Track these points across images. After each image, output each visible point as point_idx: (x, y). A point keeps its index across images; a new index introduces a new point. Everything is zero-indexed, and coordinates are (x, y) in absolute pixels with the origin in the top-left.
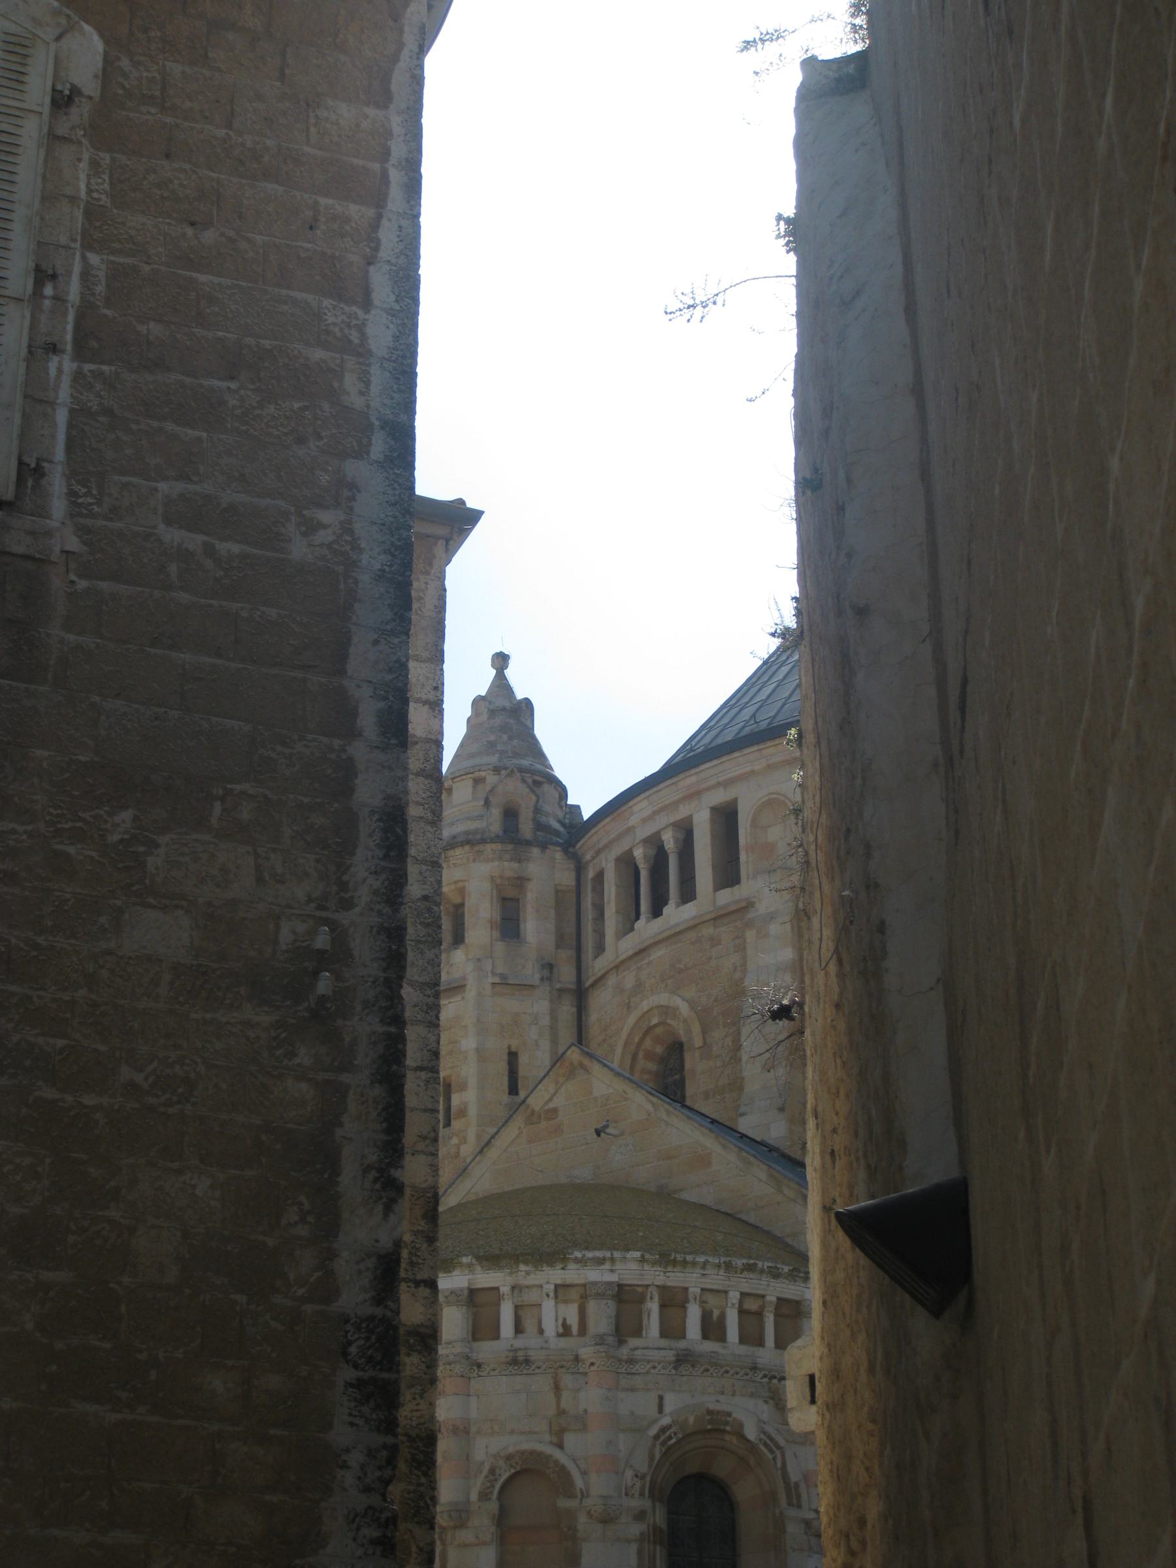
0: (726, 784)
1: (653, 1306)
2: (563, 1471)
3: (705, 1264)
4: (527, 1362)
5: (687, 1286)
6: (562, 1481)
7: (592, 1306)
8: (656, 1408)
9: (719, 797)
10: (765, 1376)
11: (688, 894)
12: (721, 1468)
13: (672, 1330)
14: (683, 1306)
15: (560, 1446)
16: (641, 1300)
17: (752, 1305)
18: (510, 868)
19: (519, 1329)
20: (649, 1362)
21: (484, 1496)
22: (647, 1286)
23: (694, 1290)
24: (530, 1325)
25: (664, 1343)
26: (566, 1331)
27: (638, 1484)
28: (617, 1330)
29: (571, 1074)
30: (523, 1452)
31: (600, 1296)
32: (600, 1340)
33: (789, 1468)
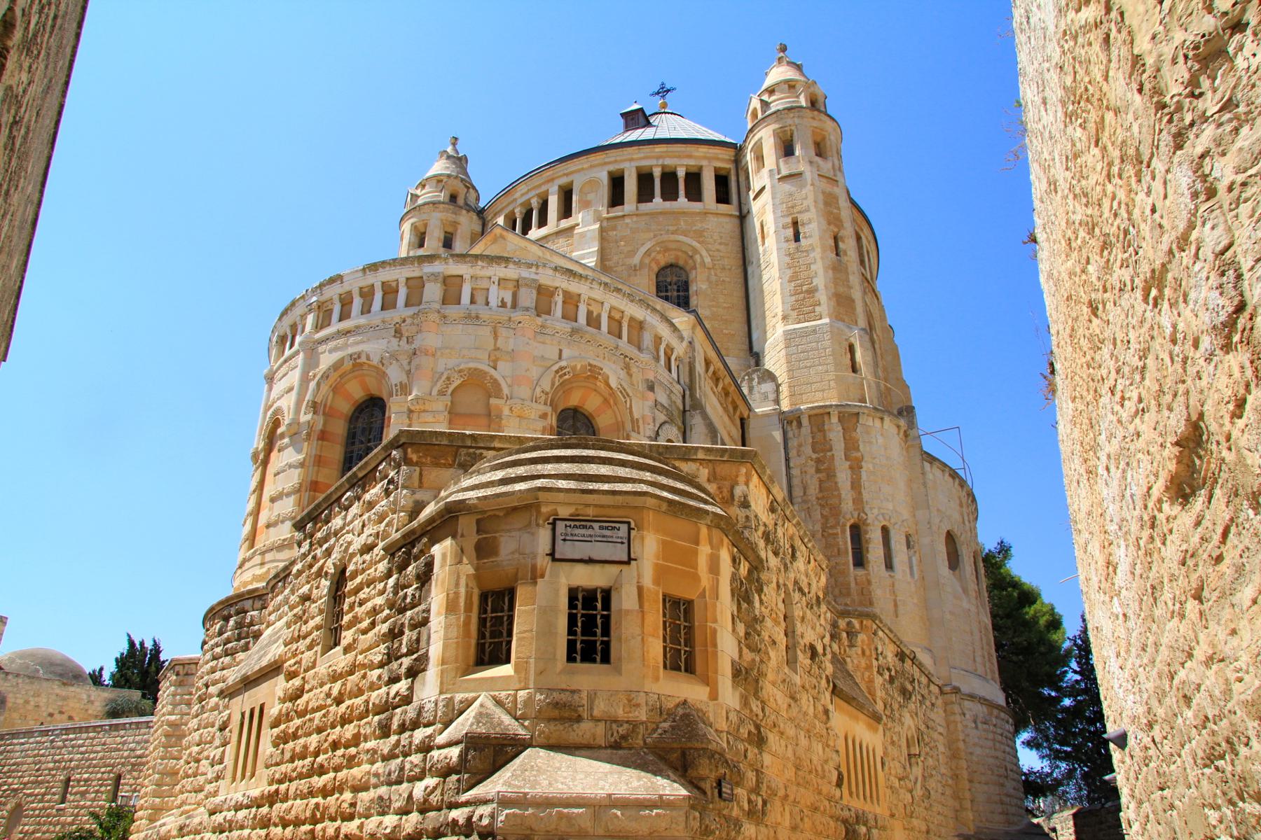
0: (567, 175)
1: (559, 299)
2: (496, 383)
4: (477, 317)
6: (493, 389)
7: (523, 292)
9: (564, 181)
11: (543, 222)
12: (591, 404)
13: (569, 316)
17: (617, 316)
18: (451, 217)
19: (473, 302)
21: (442, 393)
24: (480, 299)
26: (503, 305)
27: (543, 398)
28: (536, 308)
29: (495, 241)
30: (470, 369)
31: (526, 285)
32: (527, 309)
33: (634, 409)
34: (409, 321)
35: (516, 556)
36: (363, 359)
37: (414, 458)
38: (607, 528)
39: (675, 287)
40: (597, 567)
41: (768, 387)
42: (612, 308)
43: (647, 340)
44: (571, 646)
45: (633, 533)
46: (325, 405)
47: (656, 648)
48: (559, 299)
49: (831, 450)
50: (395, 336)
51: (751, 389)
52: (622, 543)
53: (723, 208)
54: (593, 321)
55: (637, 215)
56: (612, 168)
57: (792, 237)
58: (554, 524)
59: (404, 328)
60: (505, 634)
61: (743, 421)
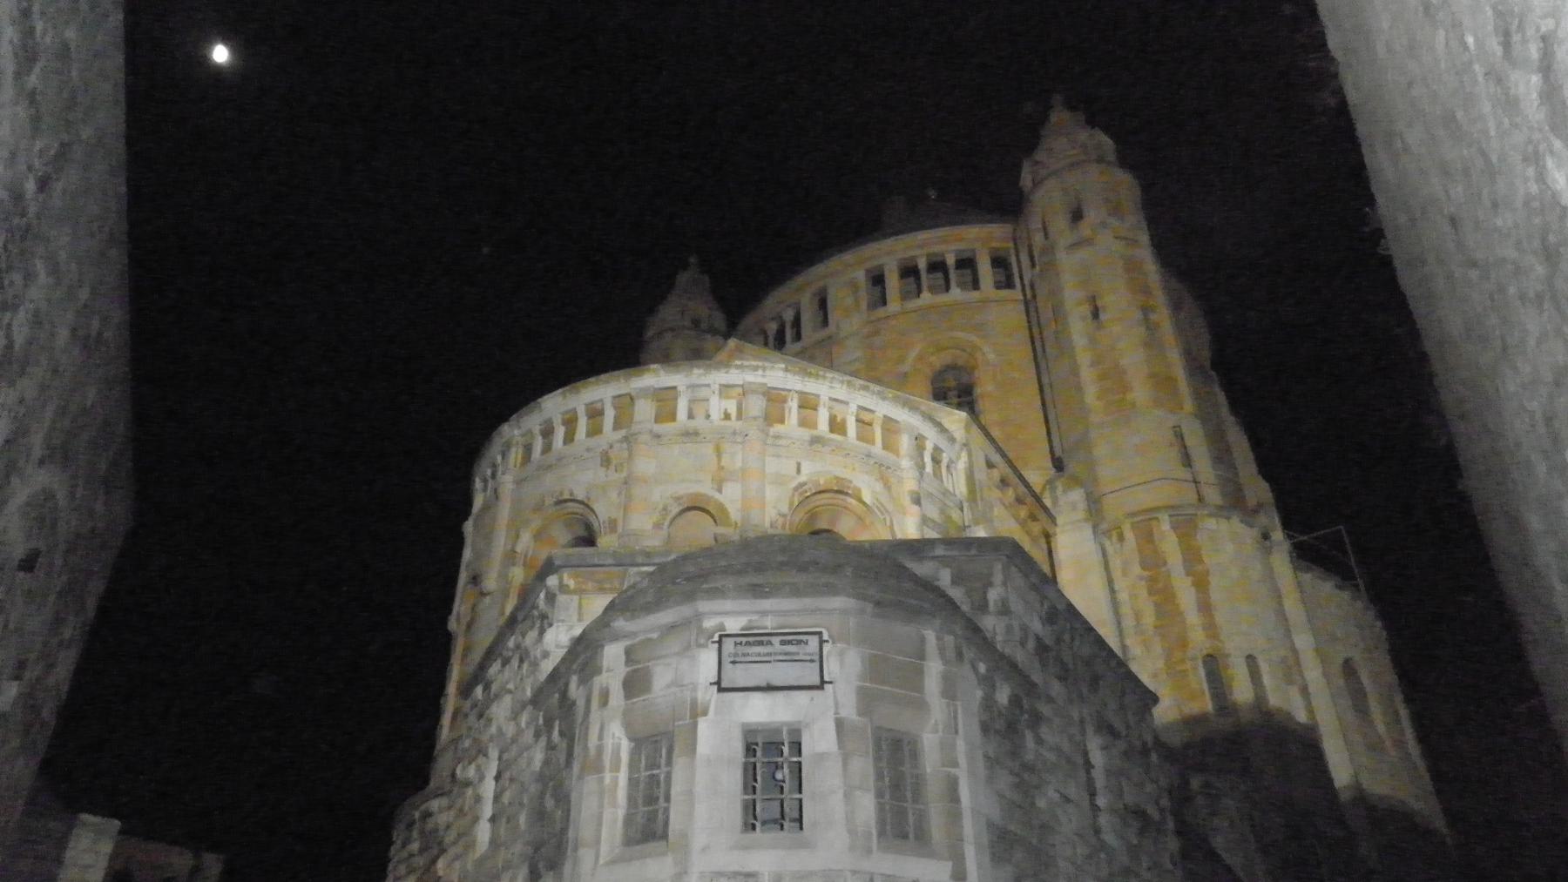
1: (793, 404)
3: (833, 378)
4: (696, 433)
5: (818, 392)
8: (795, 469)
10: (876, 463)
14: (815, 409)
15: (720, 491)
16: (784, 401)
17: (866, 417)
19: (691, 416)
20: (791, 438)
21: (658, 526)
22: (790, 391)
23: (824, 399)
24: (699, 411)
25: (802, 429)
26: (727, 416)
31: (754, 392)
32: (755, 418)
34: (617, 446)
35: (673, 689)
36: (566, 496)
37: (571, 583)
38: (790, 642)
39: (955, 393)
40: (780, 695)
41: (1077, 495)
42: (861, 408)
43: (905, 442)
44: (750, 809)
45: (826, 648)
46: (526, 556)
47: (867, 805)
48: (793, 404)
49: (1165, 563)
50: (602, 465)
51: (1055, 501)
52: (812, 661)
53: (1004, 293)
54: (837, 426)
55: (903, 313)
56: (869, 265)
57: (1089, 315)
58: (720, 642)
59: (612, 455)
60: (662, 800)
61: (1048, 537)
